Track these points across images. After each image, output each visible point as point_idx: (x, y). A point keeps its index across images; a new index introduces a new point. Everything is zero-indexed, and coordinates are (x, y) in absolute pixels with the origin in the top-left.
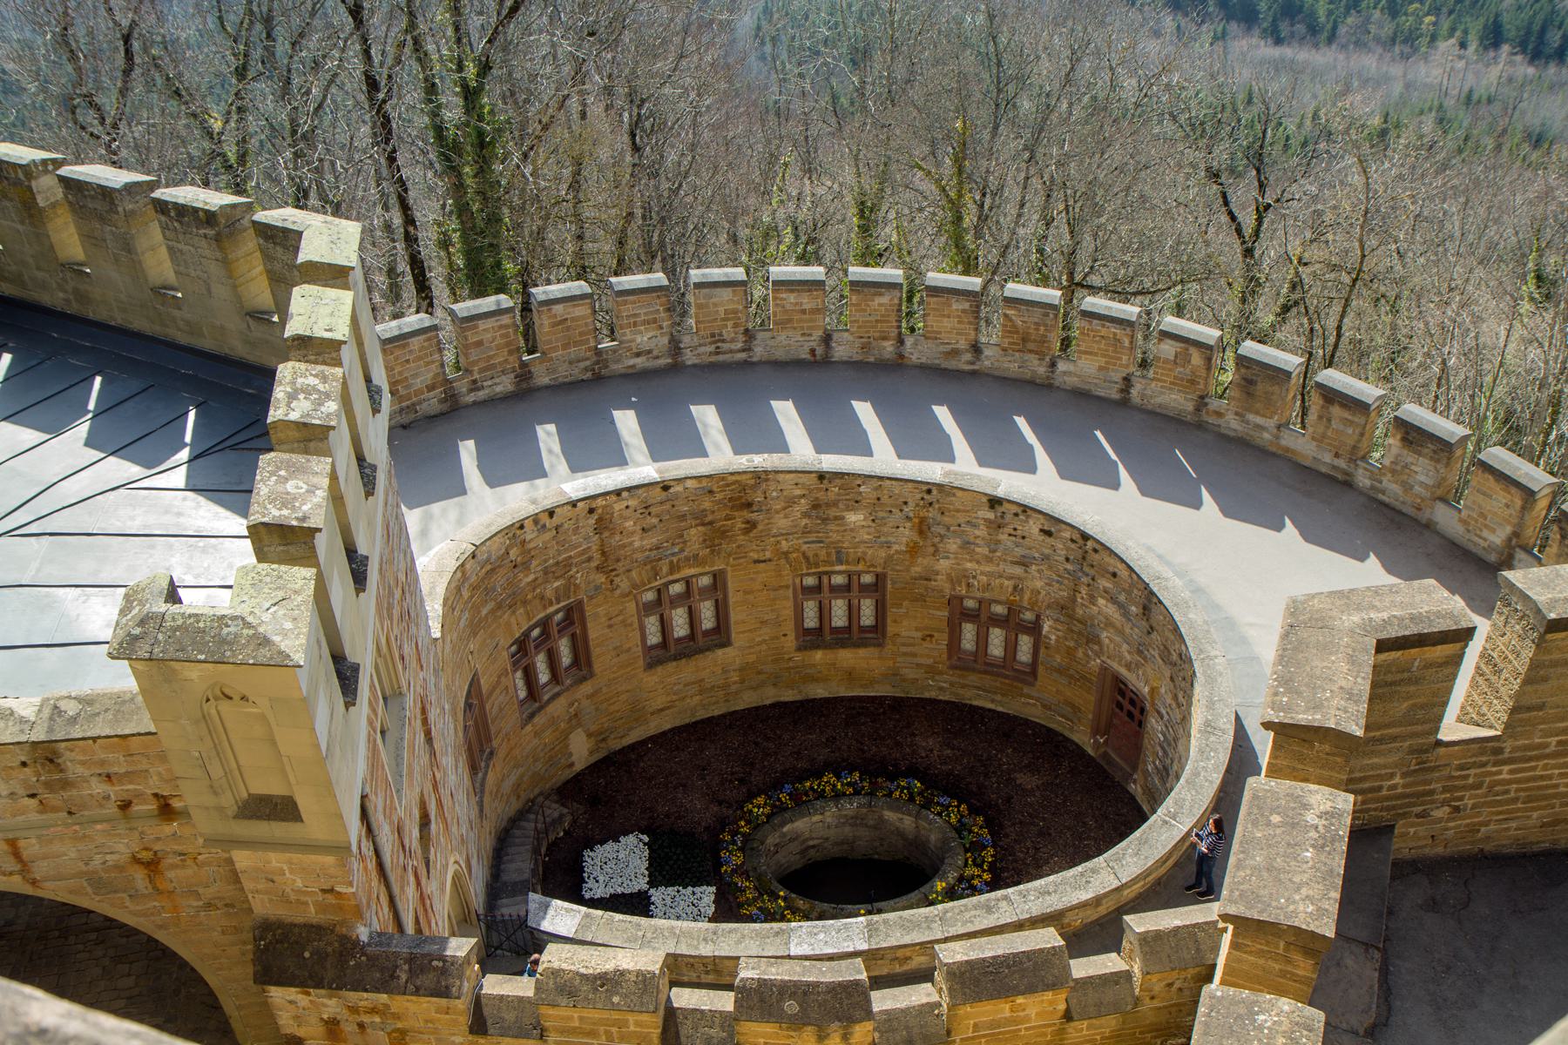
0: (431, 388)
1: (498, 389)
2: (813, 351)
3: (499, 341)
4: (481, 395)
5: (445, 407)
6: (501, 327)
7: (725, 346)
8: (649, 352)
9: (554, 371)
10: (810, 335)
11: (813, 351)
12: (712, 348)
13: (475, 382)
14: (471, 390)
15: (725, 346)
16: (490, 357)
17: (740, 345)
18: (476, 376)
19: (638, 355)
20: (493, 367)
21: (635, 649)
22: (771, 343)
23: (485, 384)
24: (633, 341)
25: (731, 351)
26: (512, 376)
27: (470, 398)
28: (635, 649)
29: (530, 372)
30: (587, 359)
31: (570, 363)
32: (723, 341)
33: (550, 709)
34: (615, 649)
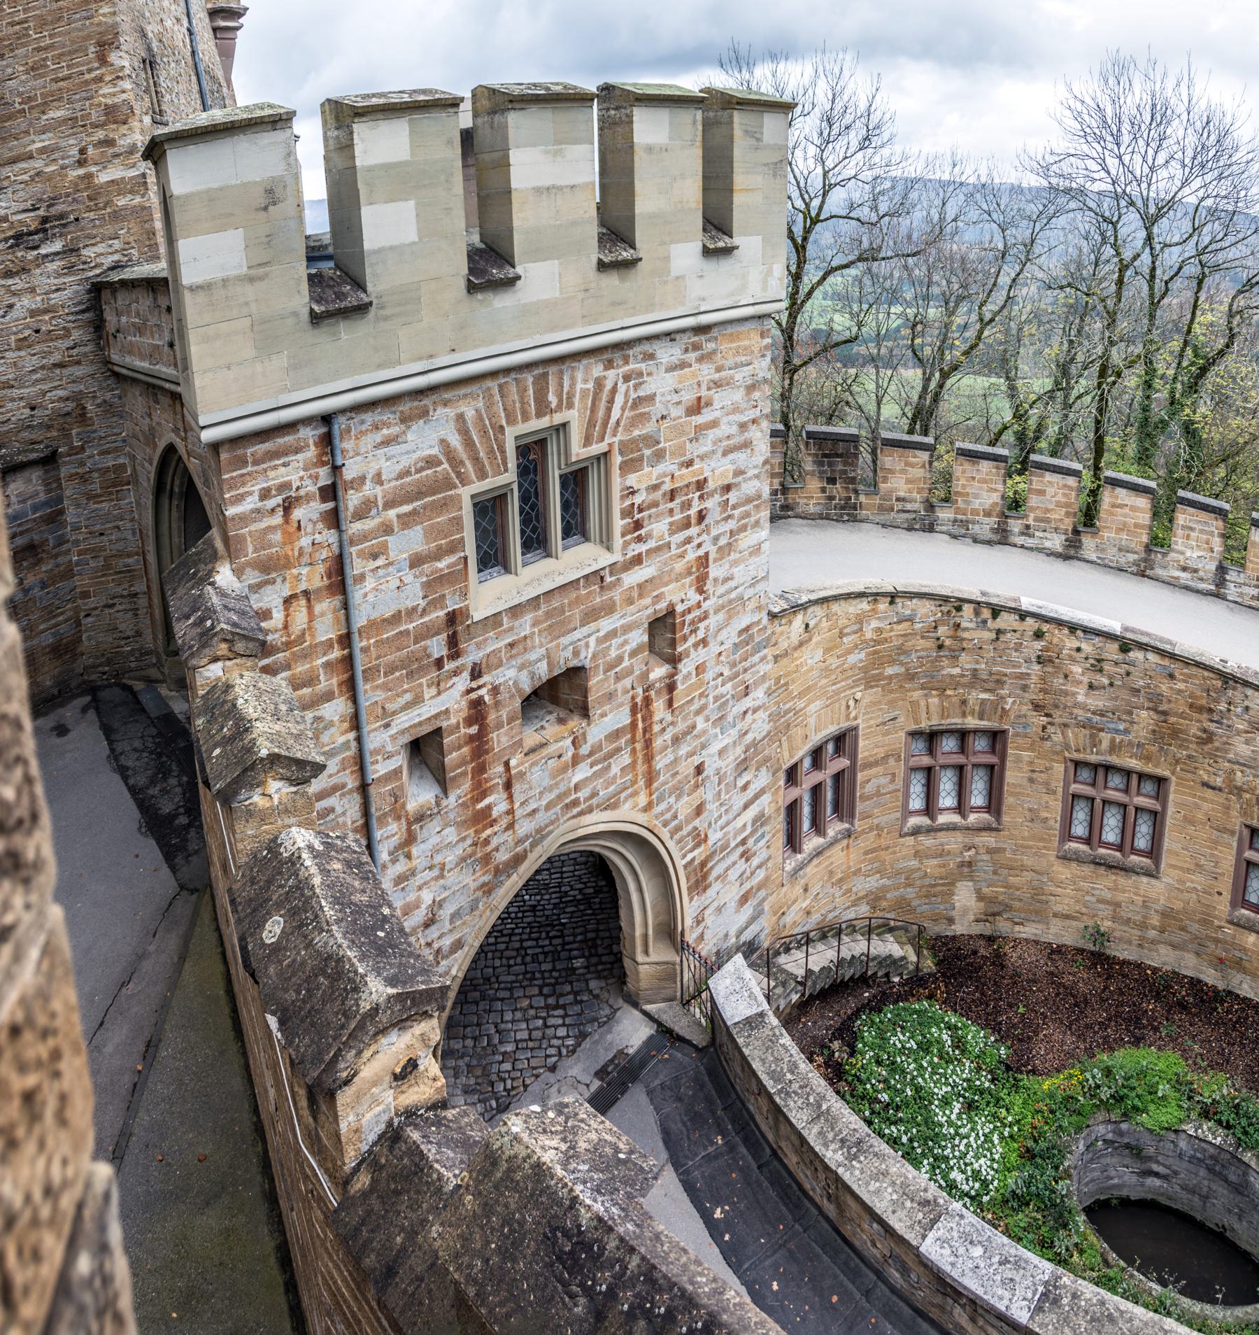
1: (1048, 544)
3: (1060, 498)
4: (1029, 542)
6: (1065, 486)
9: (1103, 550)
13: (1028, 527)
14: (1023, 534)
16: (1048, 510)
18: (1031, 522)
20: (1048, 521)
21: (1052, 822)
23: (1037, 534)
26: (1063, 537)
28: (1052, 822)
29: (1080, 541)
30: (1135, 553)
31: (1120, 550)
33: (942, 837)
34: (1030, 810)
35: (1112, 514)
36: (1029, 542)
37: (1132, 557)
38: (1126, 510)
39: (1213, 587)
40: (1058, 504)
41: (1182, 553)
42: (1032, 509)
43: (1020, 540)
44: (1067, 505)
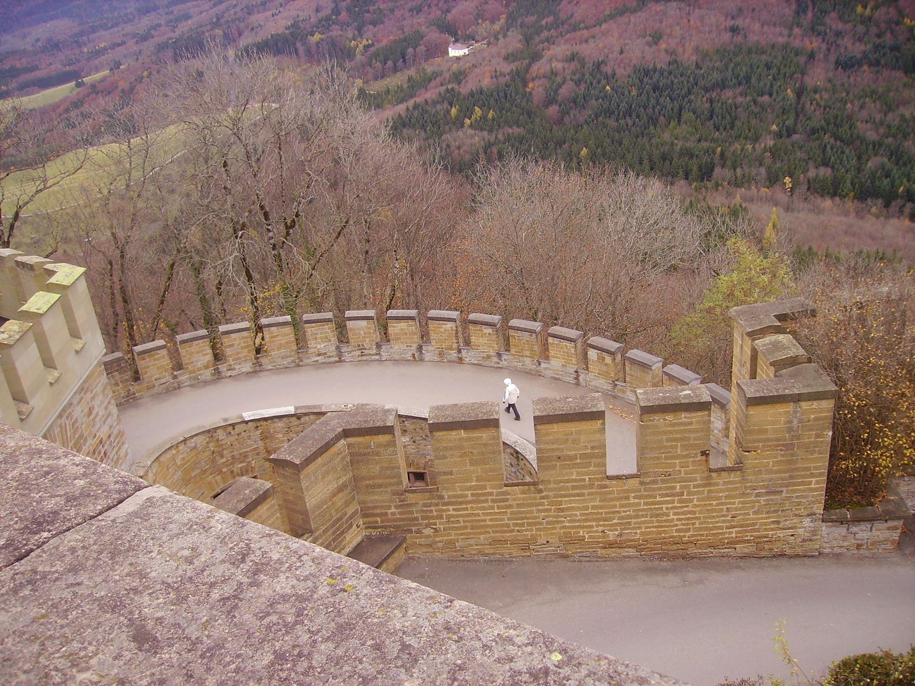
0: (206, 367)
1: (244, 370)
2: (413, 355)
5: (215, 378)
7: (366, 352)
8: (325, 354)
9: (274, 362)
10: (411, 346)
11: (413, 355)
12: (359, 353)
14: (229, 370)
15: (366, 352)
16: (238, 353)
17: (374, 352)
19: (319, 355)
20: (239, 358)
22: (392, 350)
24: (315, 348)
25: (370, 355)
27: (229, 373)
31: (282, 358)
32: (365, 349)
35: (272, 342)
36: (233, 373)
37: (290, 360)
38: (280, 338)
39: (337, 359)
40: (242, 348)
41: (315, 348)
42: (229, 356)
43: (229, 373)
44: (247, 346)
